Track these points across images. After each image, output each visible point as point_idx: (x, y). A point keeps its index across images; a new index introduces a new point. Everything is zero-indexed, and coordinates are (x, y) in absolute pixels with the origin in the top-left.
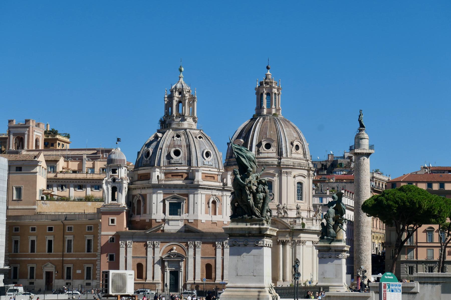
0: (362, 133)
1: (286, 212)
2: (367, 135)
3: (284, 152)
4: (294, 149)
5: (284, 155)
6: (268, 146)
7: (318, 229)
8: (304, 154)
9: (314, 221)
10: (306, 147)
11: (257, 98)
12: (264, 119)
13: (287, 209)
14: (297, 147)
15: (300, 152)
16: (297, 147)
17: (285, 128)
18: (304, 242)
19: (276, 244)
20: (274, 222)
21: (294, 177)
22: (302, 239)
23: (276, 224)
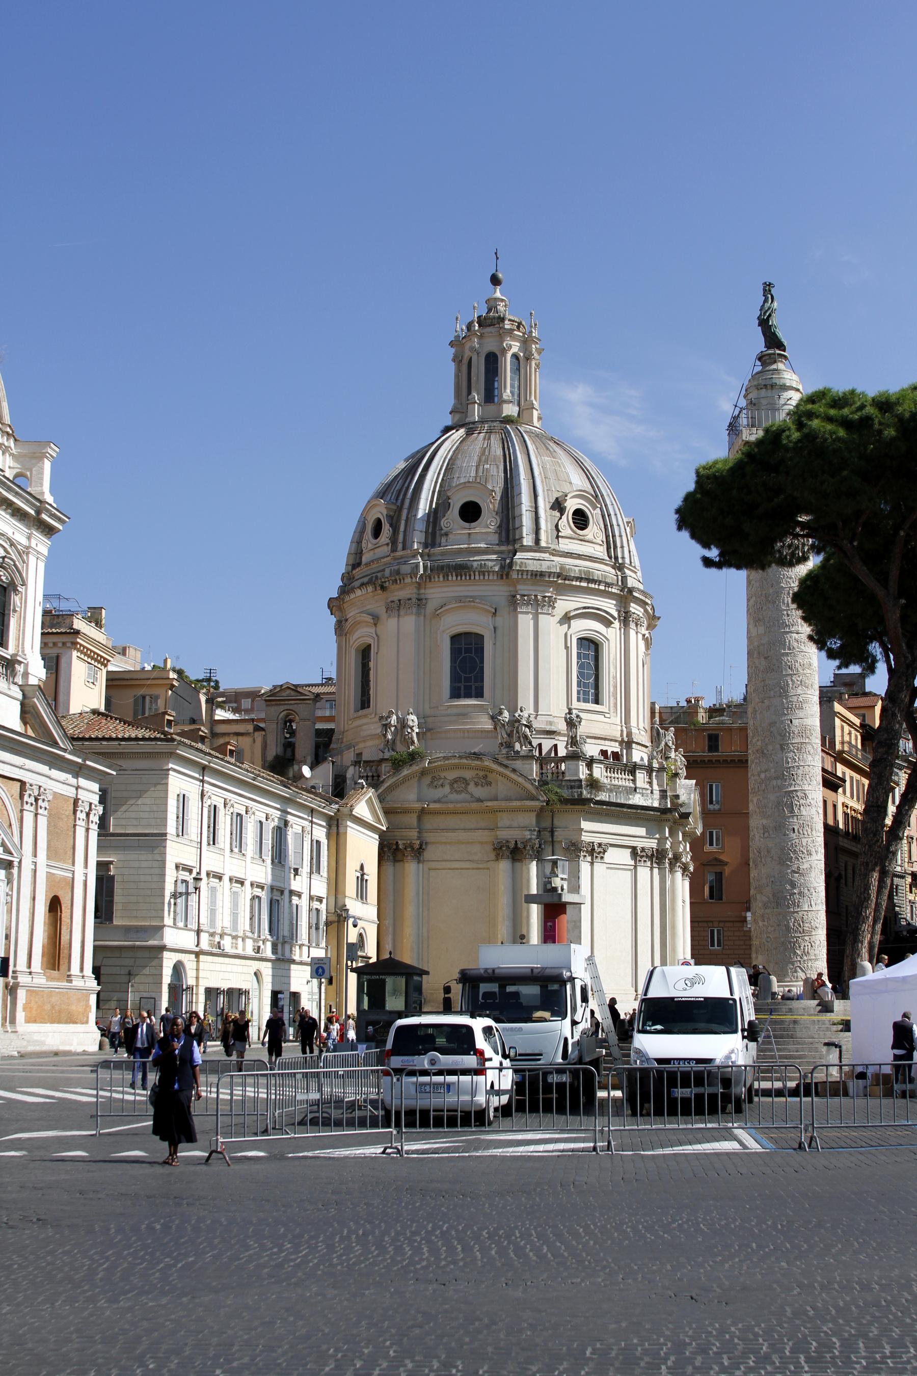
0: (774, 366)
1: (526, 737)
2: (795, 377)
3: (525, 531)
4: (566, 524)
5: (528, 541)
6: (471, 512)
7: (656, 804)
8: (610, 544)
9: (641, 776)
10: (620, 521)
11: (457, 377)
12: (469, 433)
13: (529, 727)
14: (581, 520)
15: (590, 537)
16: (581, 520)
17: (539, 454)
18: (596, 852)
19: (492, 856)
20: (485, 777)
21: (567, 619)
22: (586, 838)
23: (489, 784)
